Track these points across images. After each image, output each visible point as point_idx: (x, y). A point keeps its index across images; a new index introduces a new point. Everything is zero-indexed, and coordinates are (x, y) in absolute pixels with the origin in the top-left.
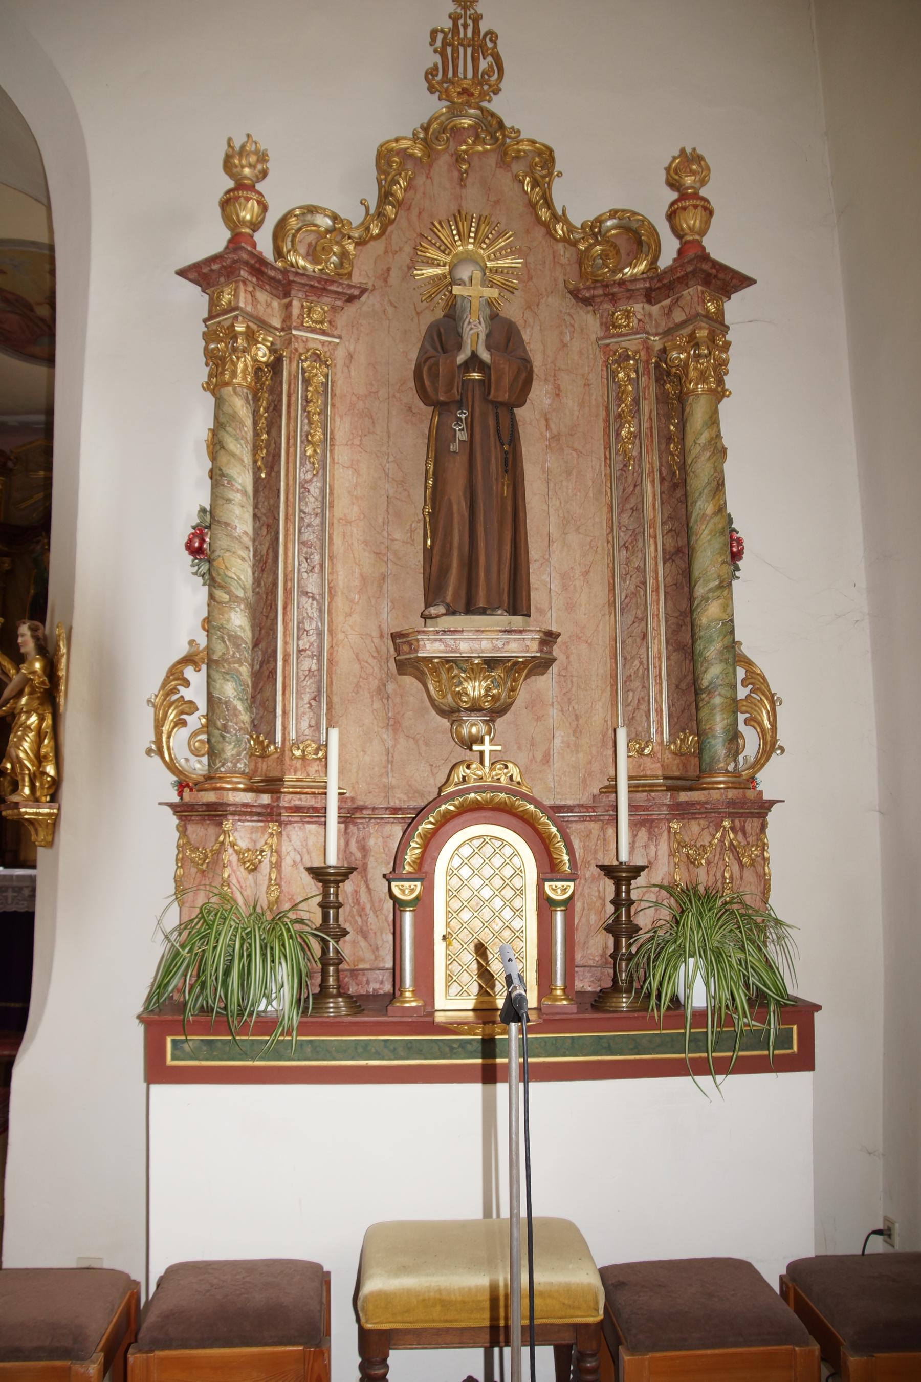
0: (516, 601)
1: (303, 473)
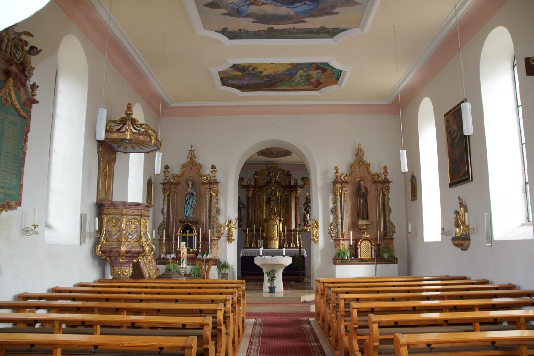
0: (367, 218)
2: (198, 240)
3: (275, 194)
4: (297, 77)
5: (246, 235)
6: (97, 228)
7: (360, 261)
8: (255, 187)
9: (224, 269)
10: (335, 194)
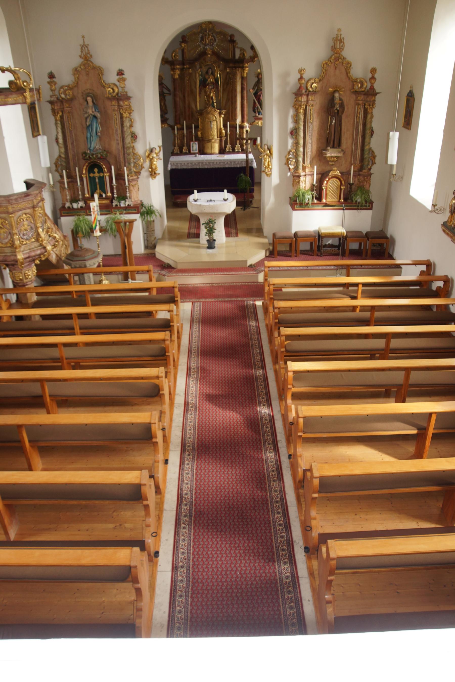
1: (309, 124)
3: (213, 74)
7: (324, 206)
8: (183, 63)
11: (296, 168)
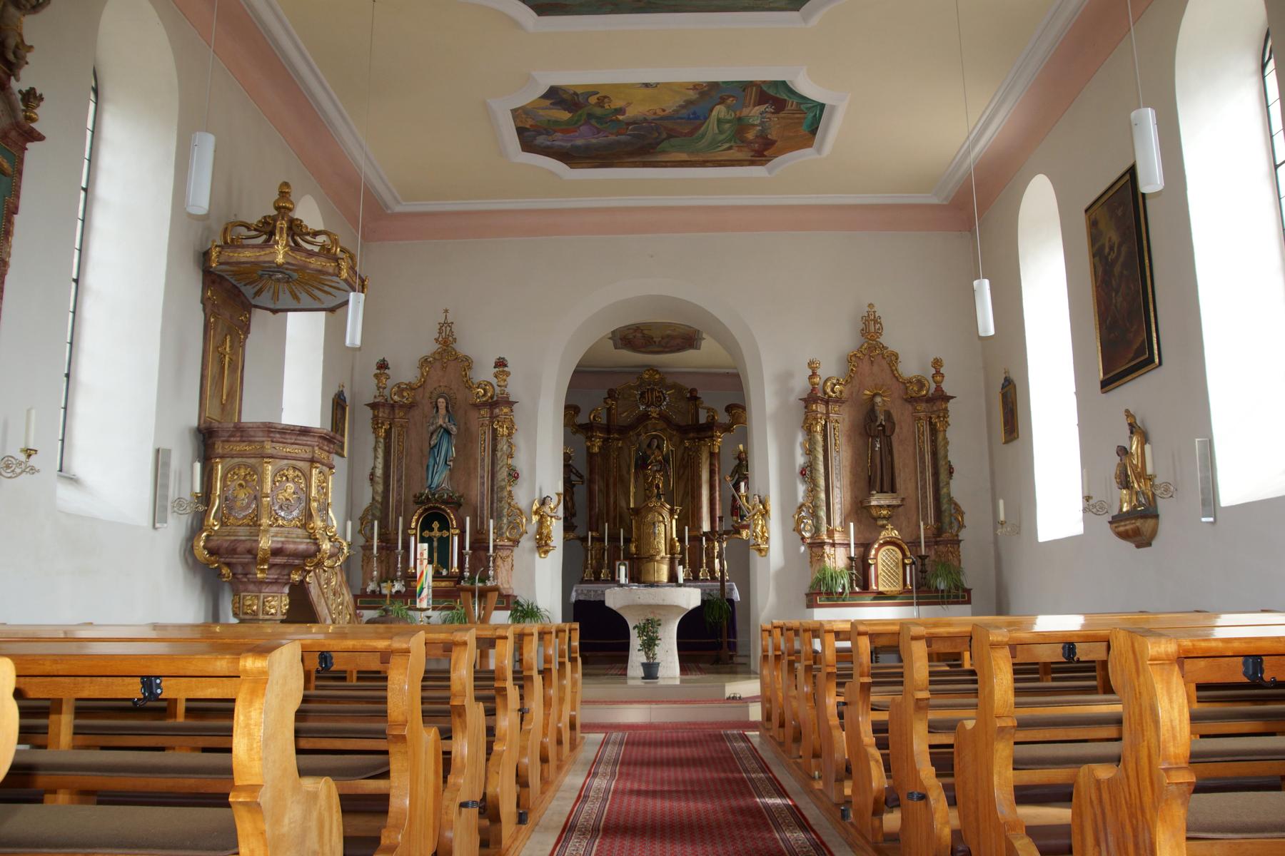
0: (893, 490)
1: (834, 454)
2: (461, 546)
3: (659, 447)
4: (711, 126)
5: (586, 550)
6: (197, 489)
7: (875, 599)
8: (608, 429)
9: (528, 620)
10: (809, 431)
11: (817, 529)
